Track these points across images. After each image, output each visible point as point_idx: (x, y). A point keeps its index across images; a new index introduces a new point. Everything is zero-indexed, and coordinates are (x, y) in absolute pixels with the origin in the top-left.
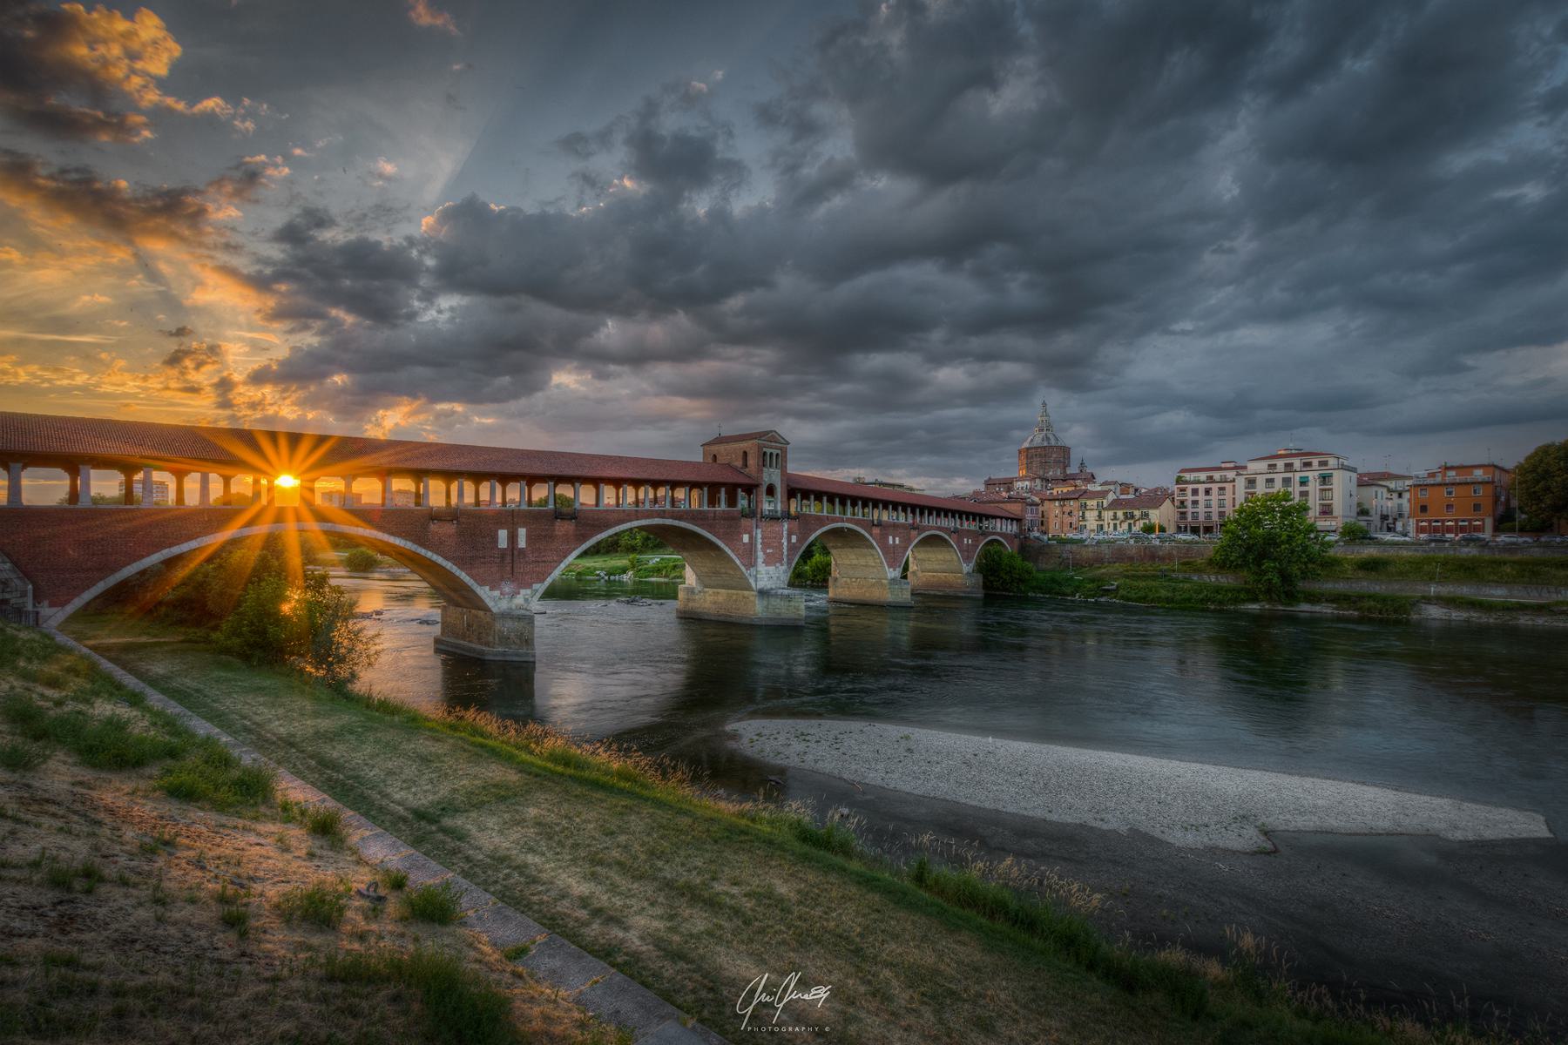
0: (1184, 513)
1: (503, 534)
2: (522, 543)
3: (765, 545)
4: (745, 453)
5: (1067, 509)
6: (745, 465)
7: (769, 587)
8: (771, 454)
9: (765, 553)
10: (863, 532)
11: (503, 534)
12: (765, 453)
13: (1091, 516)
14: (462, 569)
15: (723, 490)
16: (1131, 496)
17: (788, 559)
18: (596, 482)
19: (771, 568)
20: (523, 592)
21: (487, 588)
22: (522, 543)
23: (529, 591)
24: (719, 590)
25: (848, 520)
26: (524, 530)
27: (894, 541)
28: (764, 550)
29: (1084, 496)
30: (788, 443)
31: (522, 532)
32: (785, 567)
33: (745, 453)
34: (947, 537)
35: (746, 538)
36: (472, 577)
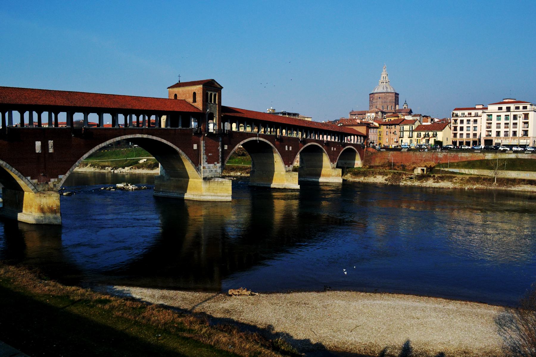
0: (456, 133)
3: (207, 151)
4: (195, 94)
5: (393, 130)
6: (195, 101)
7: (210, 176)
8: (211, 94)
9: (207, 155)
12: (207, 94)
13: (406, 134)
15: (180, 116)
16: (429, 123)
17: (222, 160)
18: (100, 112)
19: (212, 165)
24: (180, 179)
25: (261, 136)
27: (289, 148)
28: (206, 153)
29: (403, 123)
30: (222, 88)
32: (220, 165)
33: (195, 94)
34: (321, 146)
35: (195, 147)
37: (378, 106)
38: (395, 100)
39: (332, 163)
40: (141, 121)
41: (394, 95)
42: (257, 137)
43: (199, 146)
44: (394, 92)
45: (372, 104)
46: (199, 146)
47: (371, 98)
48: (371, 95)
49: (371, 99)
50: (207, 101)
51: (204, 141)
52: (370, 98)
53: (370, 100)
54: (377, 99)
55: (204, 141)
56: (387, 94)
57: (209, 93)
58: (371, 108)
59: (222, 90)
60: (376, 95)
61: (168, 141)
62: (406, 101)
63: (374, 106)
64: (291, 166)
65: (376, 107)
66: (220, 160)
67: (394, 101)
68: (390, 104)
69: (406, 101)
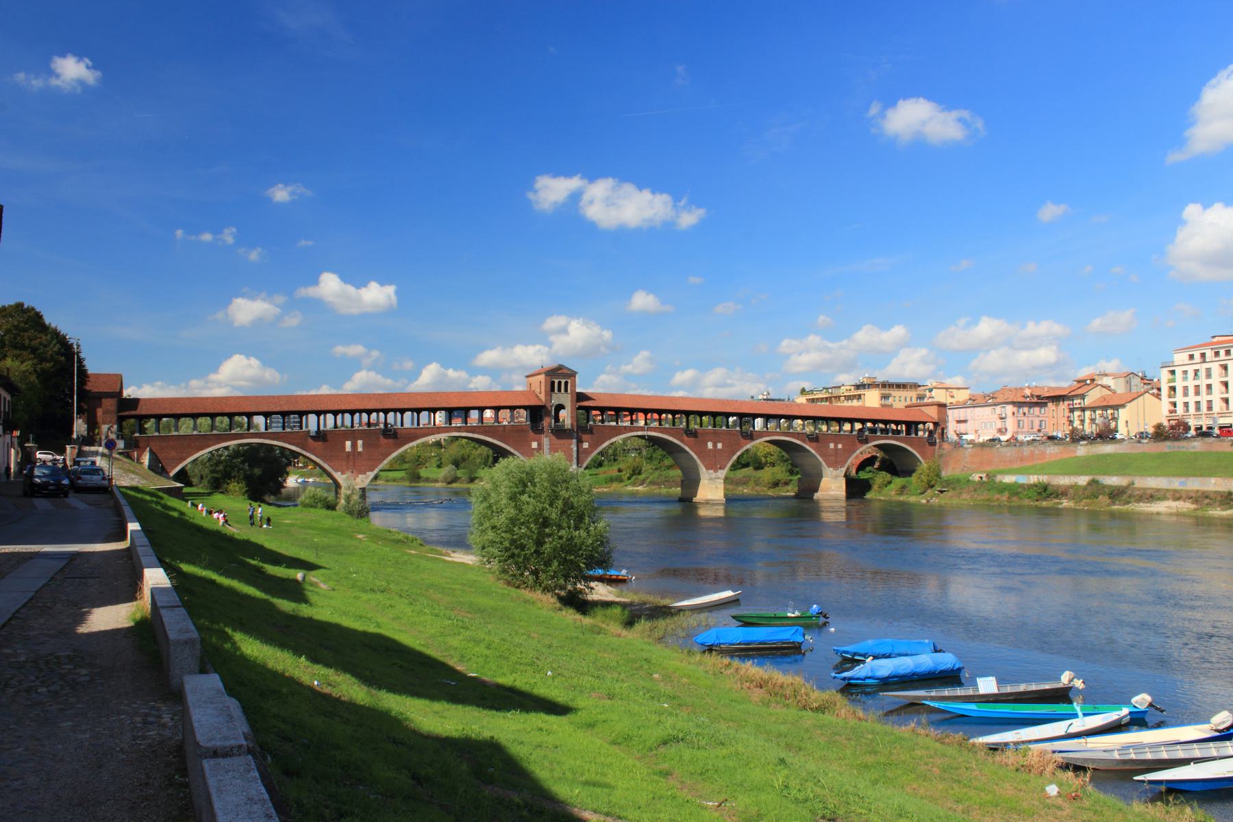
1: (348, 444)
2: (360, 449)
8: (560, 383)
10: (671, 439)
11: (348, 444)
12: (553, 383)
14: (325, 462)
20: (360, 476)
21: (339, 473)
22: (360, 449)
23: (364, 476)
26: (361, 441)
27: (715, 445)
30: (576, 373)
31: (360, 442)
36: (331, 467)
39: (831, 469)
40: (457, 417)
42: (645, 430)
43: (540, 445)
46: (540, 445)
50: (552, 389)
51: (548, 439)
55: (548, 439)
57: (556, 381)
59: (577, 376)
61: (494, 438)
64: (720, 471)
66: (575, 461)
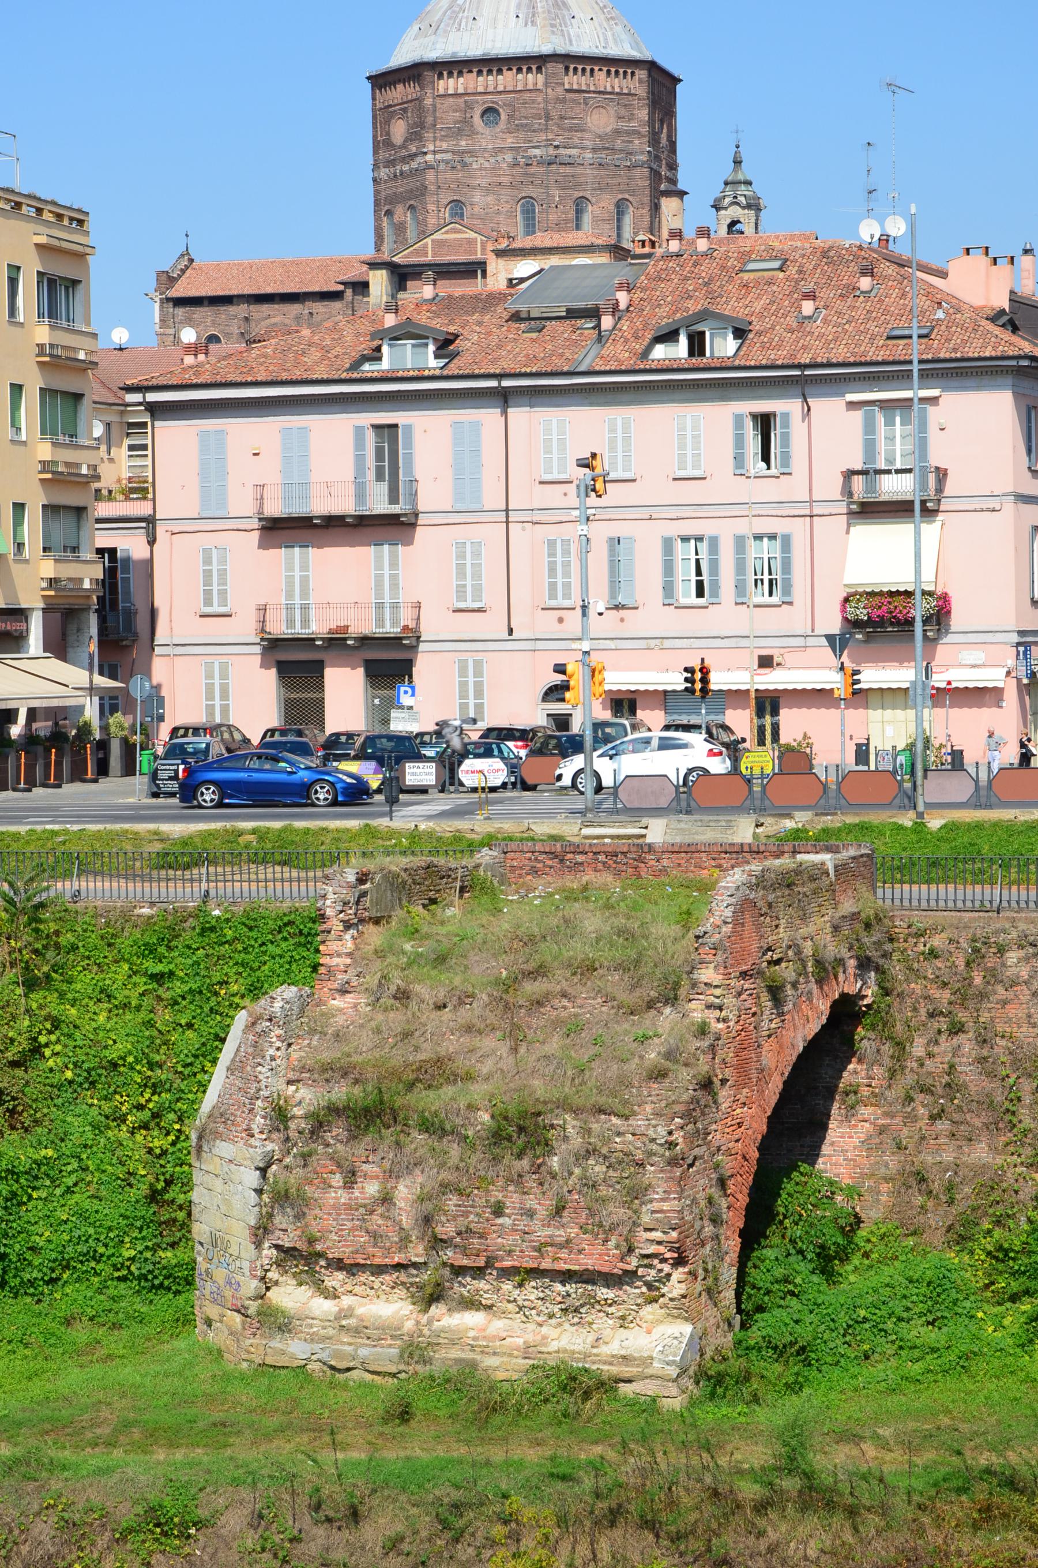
37: (479, 202)
38: (654, 140)
41: (642, 91)
44: (635, 54)
45: (401, 187)
47: (387, 122)
48: (399, 93)
49: (399, 130)
52: (382, 117)
53: (381, 143)
54: (463, 129)
56: (573, 81)
58: (400, 229)
60: (449, 85)
62: (737, 162)
63: (435, 209)
65: (457, 207)
67: (641, 147)
68: (602, 187)
69: (737, 162)
